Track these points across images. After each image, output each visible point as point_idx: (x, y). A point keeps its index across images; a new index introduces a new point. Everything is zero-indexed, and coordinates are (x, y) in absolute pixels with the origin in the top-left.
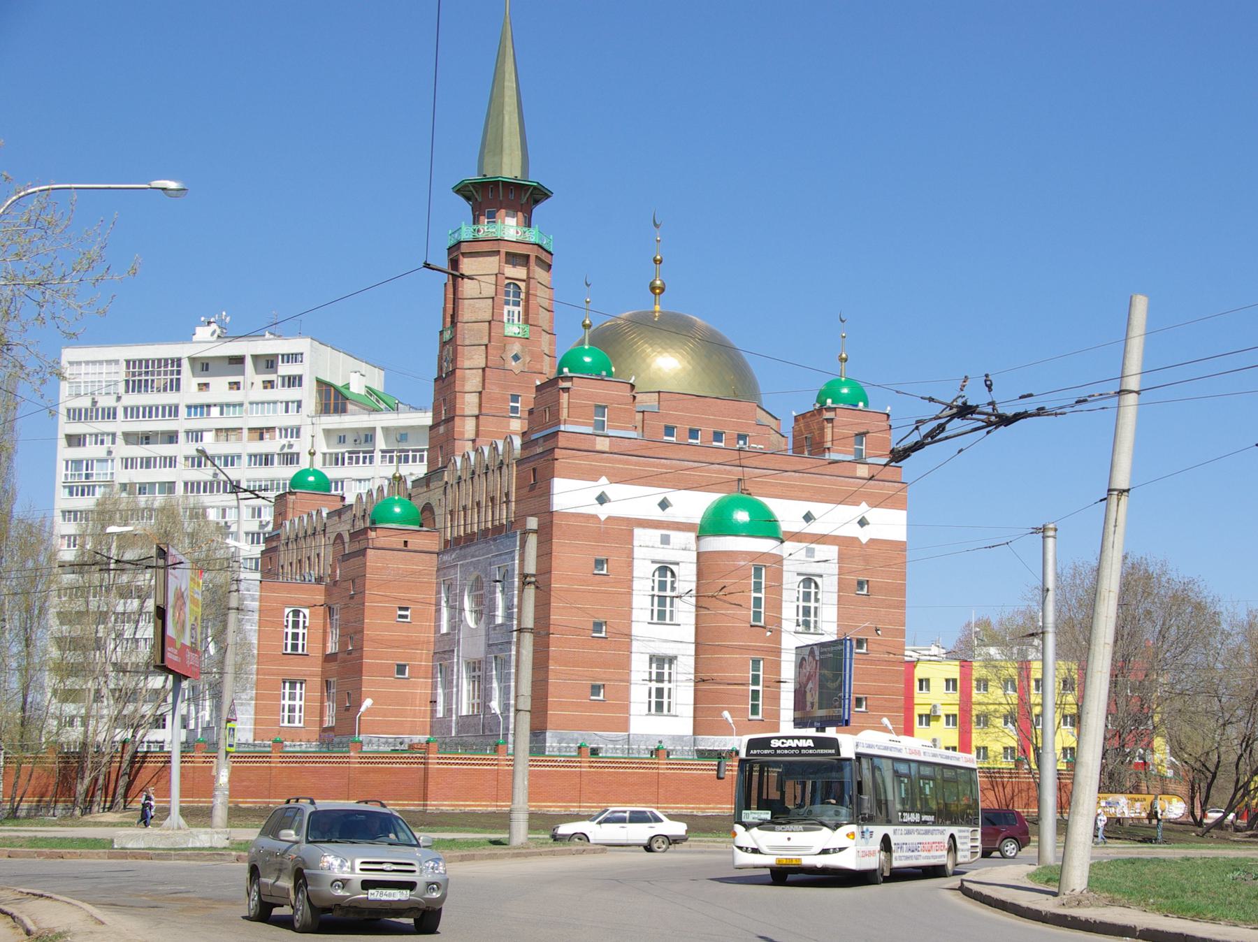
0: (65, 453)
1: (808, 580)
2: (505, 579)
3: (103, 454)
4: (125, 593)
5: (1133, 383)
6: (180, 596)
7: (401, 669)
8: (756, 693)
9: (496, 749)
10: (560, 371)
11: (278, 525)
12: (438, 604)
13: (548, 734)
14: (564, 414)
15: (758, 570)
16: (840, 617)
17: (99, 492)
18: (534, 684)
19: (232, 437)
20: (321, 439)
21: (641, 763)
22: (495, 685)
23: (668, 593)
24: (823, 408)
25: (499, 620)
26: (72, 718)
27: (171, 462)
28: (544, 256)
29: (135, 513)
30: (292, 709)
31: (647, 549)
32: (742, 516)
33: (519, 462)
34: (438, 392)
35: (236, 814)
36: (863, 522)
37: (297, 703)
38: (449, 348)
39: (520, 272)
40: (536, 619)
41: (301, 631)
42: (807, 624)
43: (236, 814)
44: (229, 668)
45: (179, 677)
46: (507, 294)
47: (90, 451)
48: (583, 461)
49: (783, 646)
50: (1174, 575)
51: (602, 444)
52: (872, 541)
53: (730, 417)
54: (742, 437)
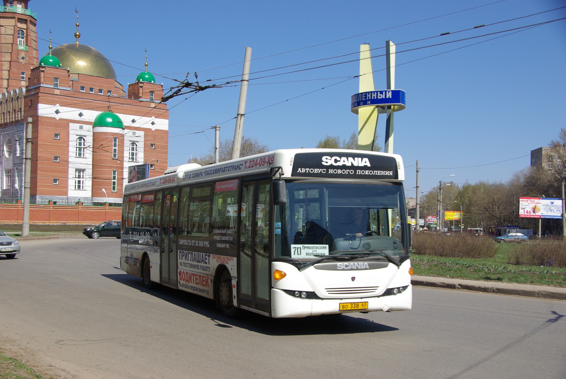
1: (133, 143)
2: (21, 139)
5: (246, 77)
8: (114, 182)
9: (17, 201)
10: (40, 64)
13: (37, 196)
15: (115, 139)
16: (145, 156)
18: (31, 178)
21: (72, 207)
22: (17, 178)
23: (82, 146)
25: (18, 155)
28: (33, 20)
31: (74, 131)
32: (109, 120)
33: (25, 97)
36: (153, 123)
39: (24, 26)
40: (32, 155)
42: (133, 158)
46: (19, 34)
48: (50, 98)
49: (124, 166)
50: (259, 144)
51: (57, 92)
52: (156, 130)
53: (106, 84)
54: (109, 91)
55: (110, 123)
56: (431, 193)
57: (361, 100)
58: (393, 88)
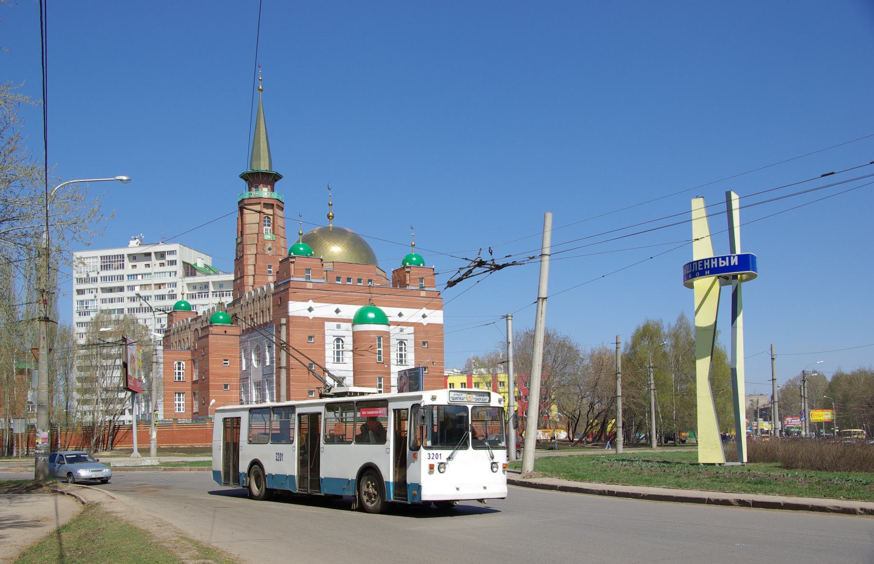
0: (77, 297)
1: (401, 342)
3: (93, 298)
4: (109, 357)
6: (133, 357)
7: (226, 386)
10: (290, 254)
11: (169, 326)
12: (241, 357)
14: (292, 273)
15: (379, 339)
17: (93, 315)
19: (147, 288)
20: (186, 287)
22: (267, 392)
24: (405, 267)
26: (85, 413)
27: (121, 300)
28: (280, 204)
29: (109, 322)
30: (179, 405)
32: (371, 315)
33: (274, 295)
34: (236, 265)
35: (160, 451)
37: (182, 402)
38: (240, 246)
39: (270, 212)
41: (181, 371)
43: (160, 451)
44: (154, 388)
45: (134, 393)
47: (87, 296)
48: (301, 293)
50: (559, 334)
51: (309, 286)
54: (370, 281)
55: (373, 319)
56: (787, 387)
57: (696, 270)
58: (738, 252)
